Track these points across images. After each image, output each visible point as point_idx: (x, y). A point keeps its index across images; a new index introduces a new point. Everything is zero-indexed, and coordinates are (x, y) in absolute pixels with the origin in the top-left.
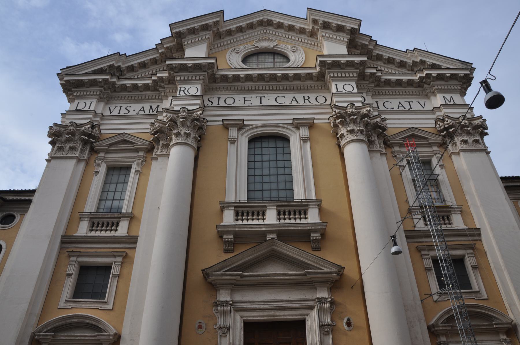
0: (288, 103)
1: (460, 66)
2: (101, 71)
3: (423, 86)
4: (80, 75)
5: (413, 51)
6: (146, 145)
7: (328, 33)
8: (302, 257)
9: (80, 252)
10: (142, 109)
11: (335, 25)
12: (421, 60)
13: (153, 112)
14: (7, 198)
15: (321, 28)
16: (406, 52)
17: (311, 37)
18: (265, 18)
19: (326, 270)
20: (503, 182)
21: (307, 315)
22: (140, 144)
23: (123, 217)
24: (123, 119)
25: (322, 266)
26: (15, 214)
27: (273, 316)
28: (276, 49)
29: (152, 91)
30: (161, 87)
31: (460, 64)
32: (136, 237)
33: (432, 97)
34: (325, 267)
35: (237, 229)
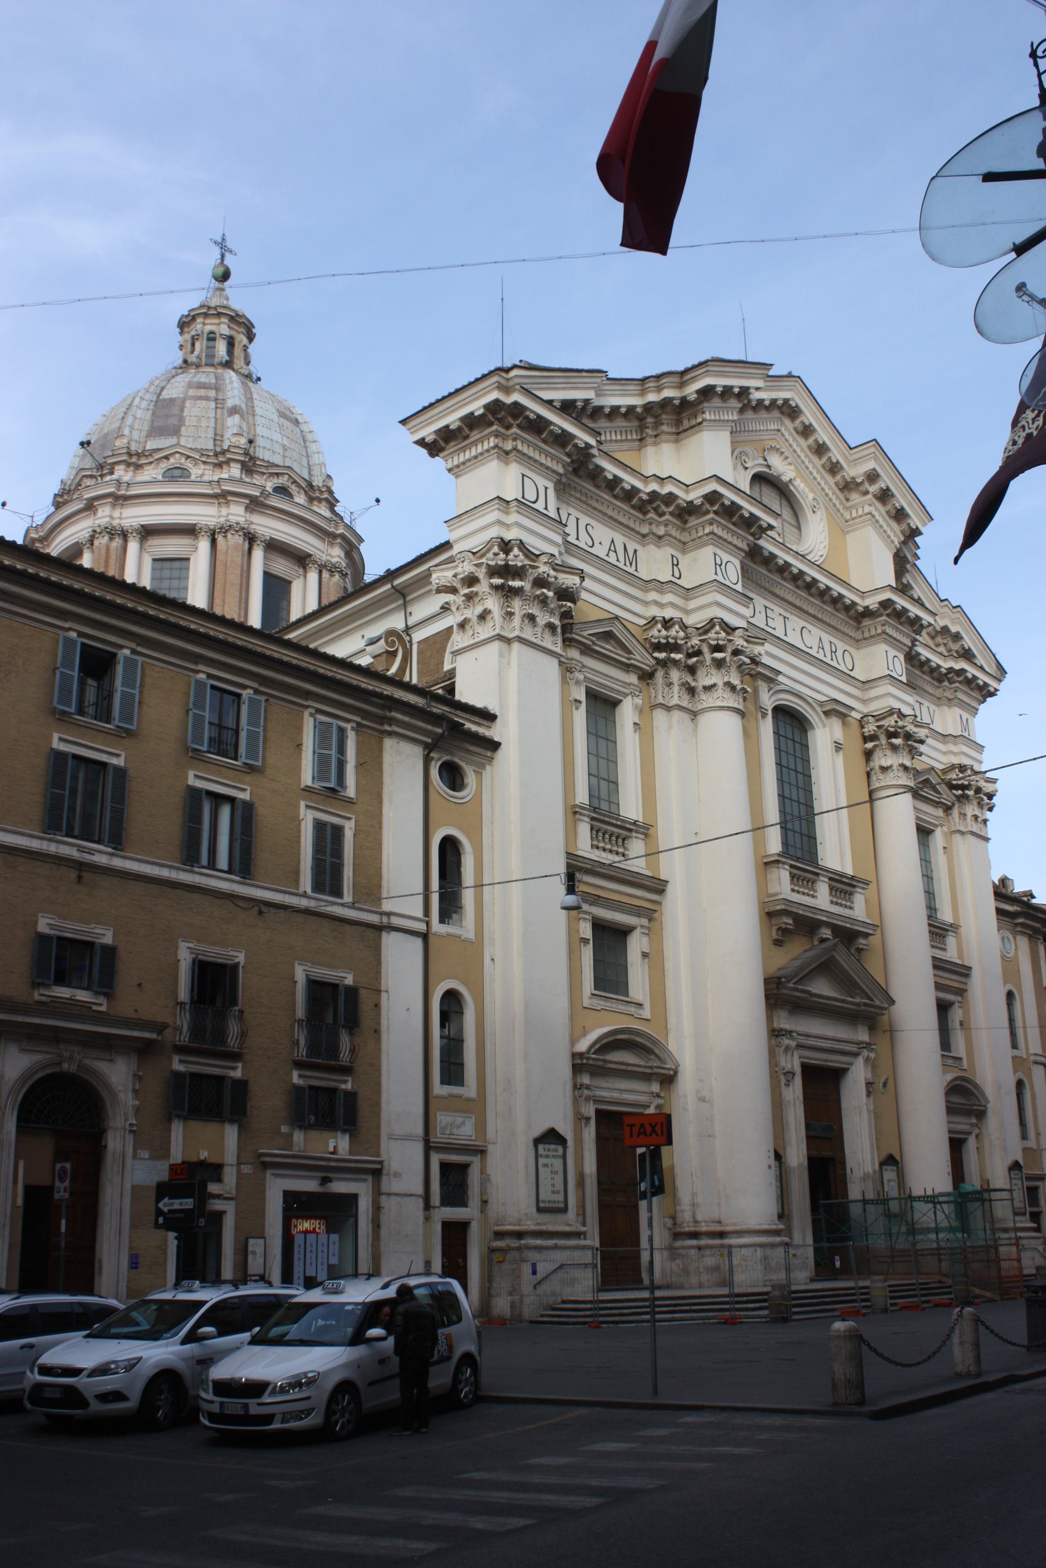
0: (813, 652)
1: (991, 668)
2: (567, 408)
3: (944, 681)
4: (531, 396)
5: (954, 607)
6: (648, 666)
7: (879, 511)
8: (859, 977)
9: (599, 896)
10: (612, 548)
11: (897, 505)
12: (958, 633)
13: (631, 564)
14: (468, 725)
15: (875, 496)
16: (942, 601)
17: (841, 490)
18: (793, 399)
19: (877, 1003)
20: (995, 899)
21: (852, 1064)
22: (638, 658)
23: (637, 832)
24: (605, 572)
25: (875, 996)
26: (463, 764)
27: (826, 1061)
28: (792, 488)
29: (633, 507)
30: (656, 510)
31: (994, 667)
32: (664, 883)
33: (945, 708)
34: (878, 999)
35: (801, 912)
